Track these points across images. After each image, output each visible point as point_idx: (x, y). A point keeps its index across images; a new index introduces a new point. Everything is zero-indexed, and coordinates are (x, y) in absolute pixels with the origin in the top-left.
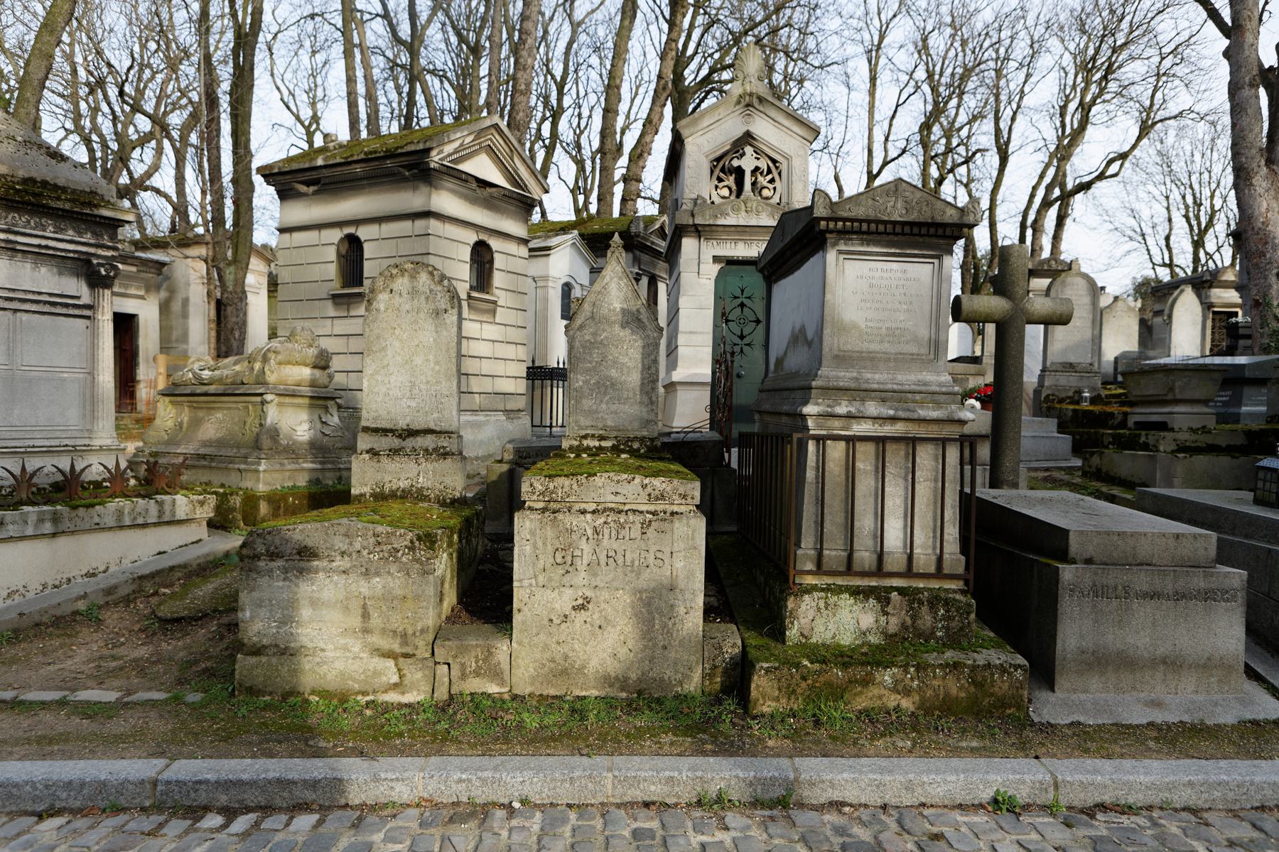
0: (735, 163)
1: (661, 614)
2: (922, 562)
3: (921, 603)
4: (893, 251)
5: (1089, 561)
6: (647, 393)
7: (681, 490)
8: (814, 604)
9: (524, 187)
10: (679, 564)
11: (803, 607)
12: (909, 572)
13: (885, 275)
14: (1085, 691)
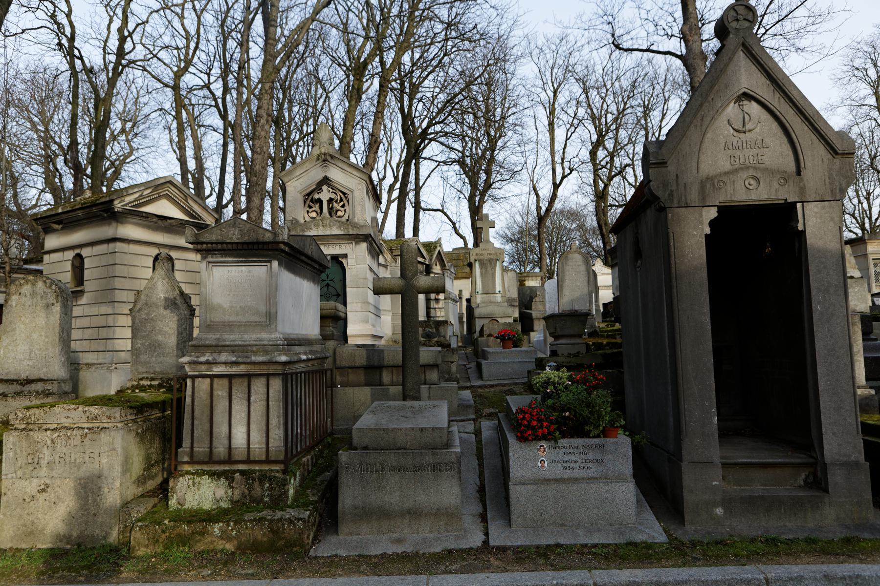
0: (316, 196)
1: (93, 493)
2: (257, 453)
3: (254, 480)
5: (365, 448)
7: (108, 414)
8: (186, 483)
9: (200, 218)
10: (104, 461)
11: (179, 485)
12: (248, 461)
14: (359, 534)
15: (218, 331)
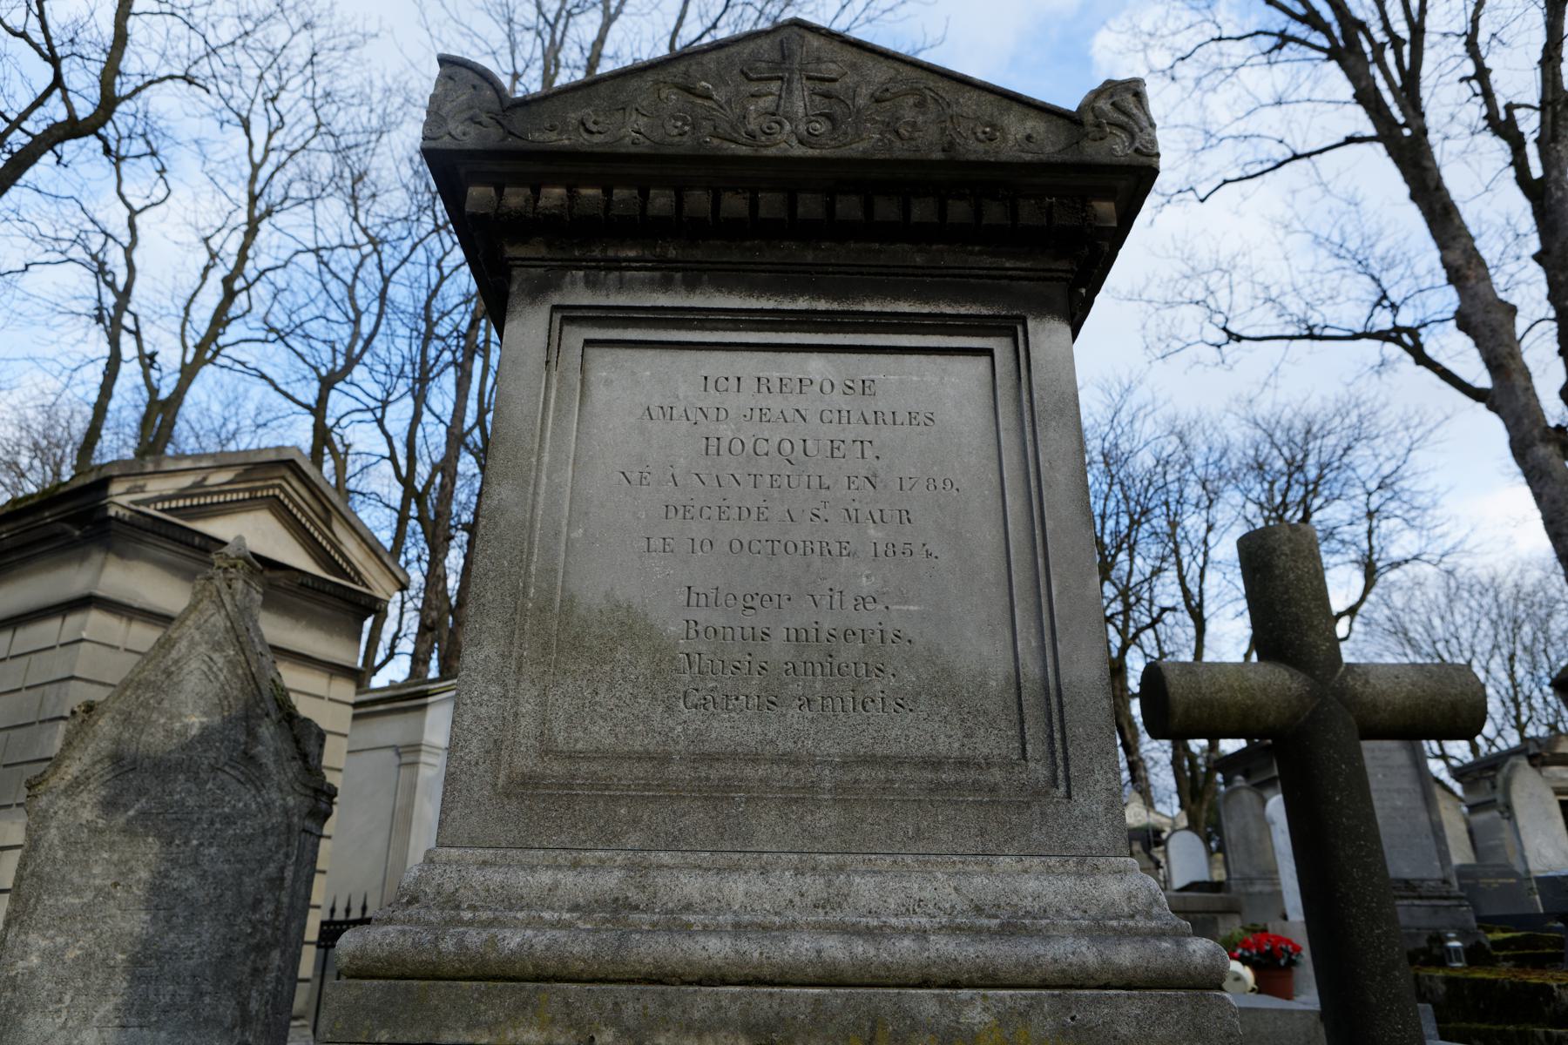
4: (802, 304)
6: (237, 986)
9: (358, 577)
13: (775, 403)
15: (609, 838)
